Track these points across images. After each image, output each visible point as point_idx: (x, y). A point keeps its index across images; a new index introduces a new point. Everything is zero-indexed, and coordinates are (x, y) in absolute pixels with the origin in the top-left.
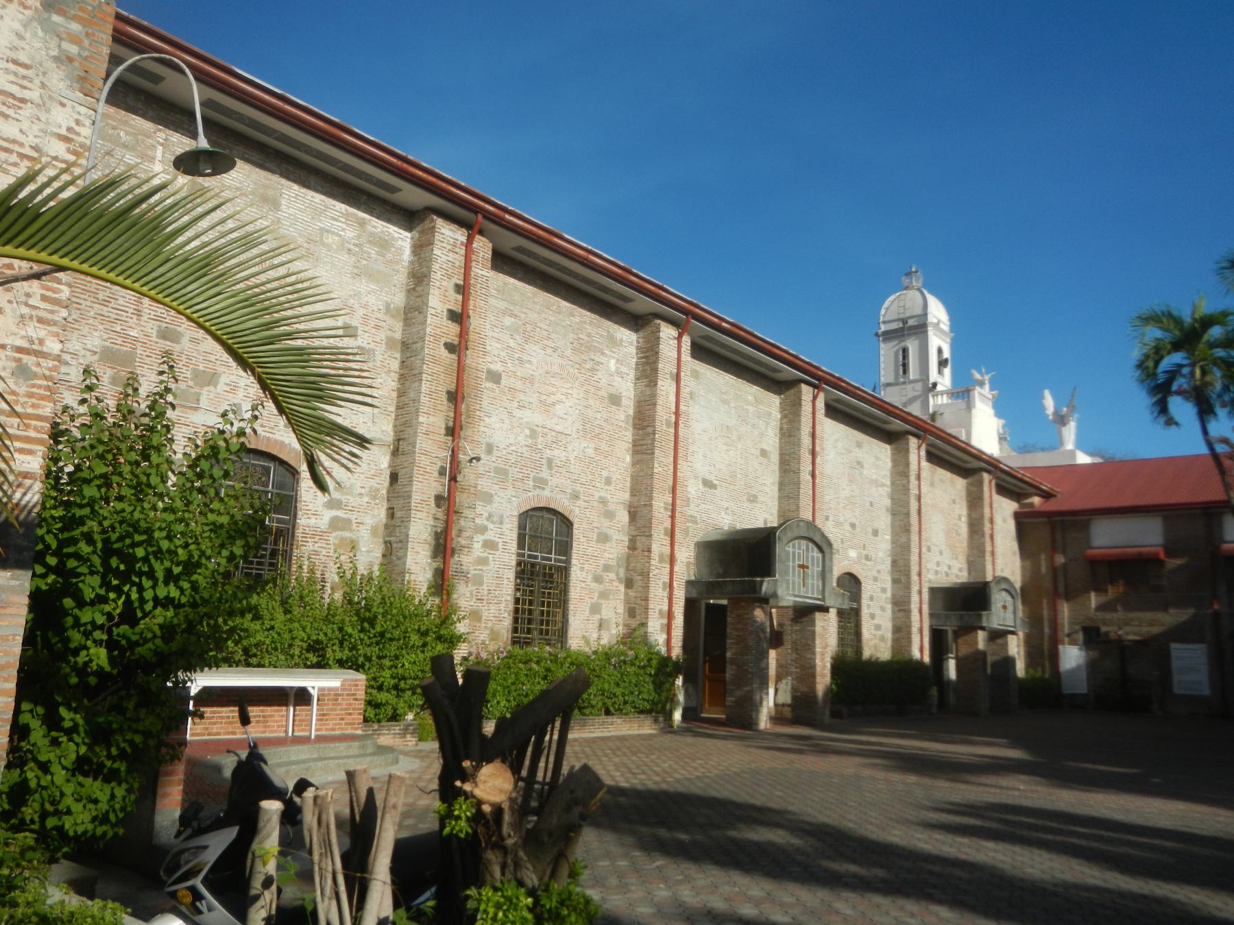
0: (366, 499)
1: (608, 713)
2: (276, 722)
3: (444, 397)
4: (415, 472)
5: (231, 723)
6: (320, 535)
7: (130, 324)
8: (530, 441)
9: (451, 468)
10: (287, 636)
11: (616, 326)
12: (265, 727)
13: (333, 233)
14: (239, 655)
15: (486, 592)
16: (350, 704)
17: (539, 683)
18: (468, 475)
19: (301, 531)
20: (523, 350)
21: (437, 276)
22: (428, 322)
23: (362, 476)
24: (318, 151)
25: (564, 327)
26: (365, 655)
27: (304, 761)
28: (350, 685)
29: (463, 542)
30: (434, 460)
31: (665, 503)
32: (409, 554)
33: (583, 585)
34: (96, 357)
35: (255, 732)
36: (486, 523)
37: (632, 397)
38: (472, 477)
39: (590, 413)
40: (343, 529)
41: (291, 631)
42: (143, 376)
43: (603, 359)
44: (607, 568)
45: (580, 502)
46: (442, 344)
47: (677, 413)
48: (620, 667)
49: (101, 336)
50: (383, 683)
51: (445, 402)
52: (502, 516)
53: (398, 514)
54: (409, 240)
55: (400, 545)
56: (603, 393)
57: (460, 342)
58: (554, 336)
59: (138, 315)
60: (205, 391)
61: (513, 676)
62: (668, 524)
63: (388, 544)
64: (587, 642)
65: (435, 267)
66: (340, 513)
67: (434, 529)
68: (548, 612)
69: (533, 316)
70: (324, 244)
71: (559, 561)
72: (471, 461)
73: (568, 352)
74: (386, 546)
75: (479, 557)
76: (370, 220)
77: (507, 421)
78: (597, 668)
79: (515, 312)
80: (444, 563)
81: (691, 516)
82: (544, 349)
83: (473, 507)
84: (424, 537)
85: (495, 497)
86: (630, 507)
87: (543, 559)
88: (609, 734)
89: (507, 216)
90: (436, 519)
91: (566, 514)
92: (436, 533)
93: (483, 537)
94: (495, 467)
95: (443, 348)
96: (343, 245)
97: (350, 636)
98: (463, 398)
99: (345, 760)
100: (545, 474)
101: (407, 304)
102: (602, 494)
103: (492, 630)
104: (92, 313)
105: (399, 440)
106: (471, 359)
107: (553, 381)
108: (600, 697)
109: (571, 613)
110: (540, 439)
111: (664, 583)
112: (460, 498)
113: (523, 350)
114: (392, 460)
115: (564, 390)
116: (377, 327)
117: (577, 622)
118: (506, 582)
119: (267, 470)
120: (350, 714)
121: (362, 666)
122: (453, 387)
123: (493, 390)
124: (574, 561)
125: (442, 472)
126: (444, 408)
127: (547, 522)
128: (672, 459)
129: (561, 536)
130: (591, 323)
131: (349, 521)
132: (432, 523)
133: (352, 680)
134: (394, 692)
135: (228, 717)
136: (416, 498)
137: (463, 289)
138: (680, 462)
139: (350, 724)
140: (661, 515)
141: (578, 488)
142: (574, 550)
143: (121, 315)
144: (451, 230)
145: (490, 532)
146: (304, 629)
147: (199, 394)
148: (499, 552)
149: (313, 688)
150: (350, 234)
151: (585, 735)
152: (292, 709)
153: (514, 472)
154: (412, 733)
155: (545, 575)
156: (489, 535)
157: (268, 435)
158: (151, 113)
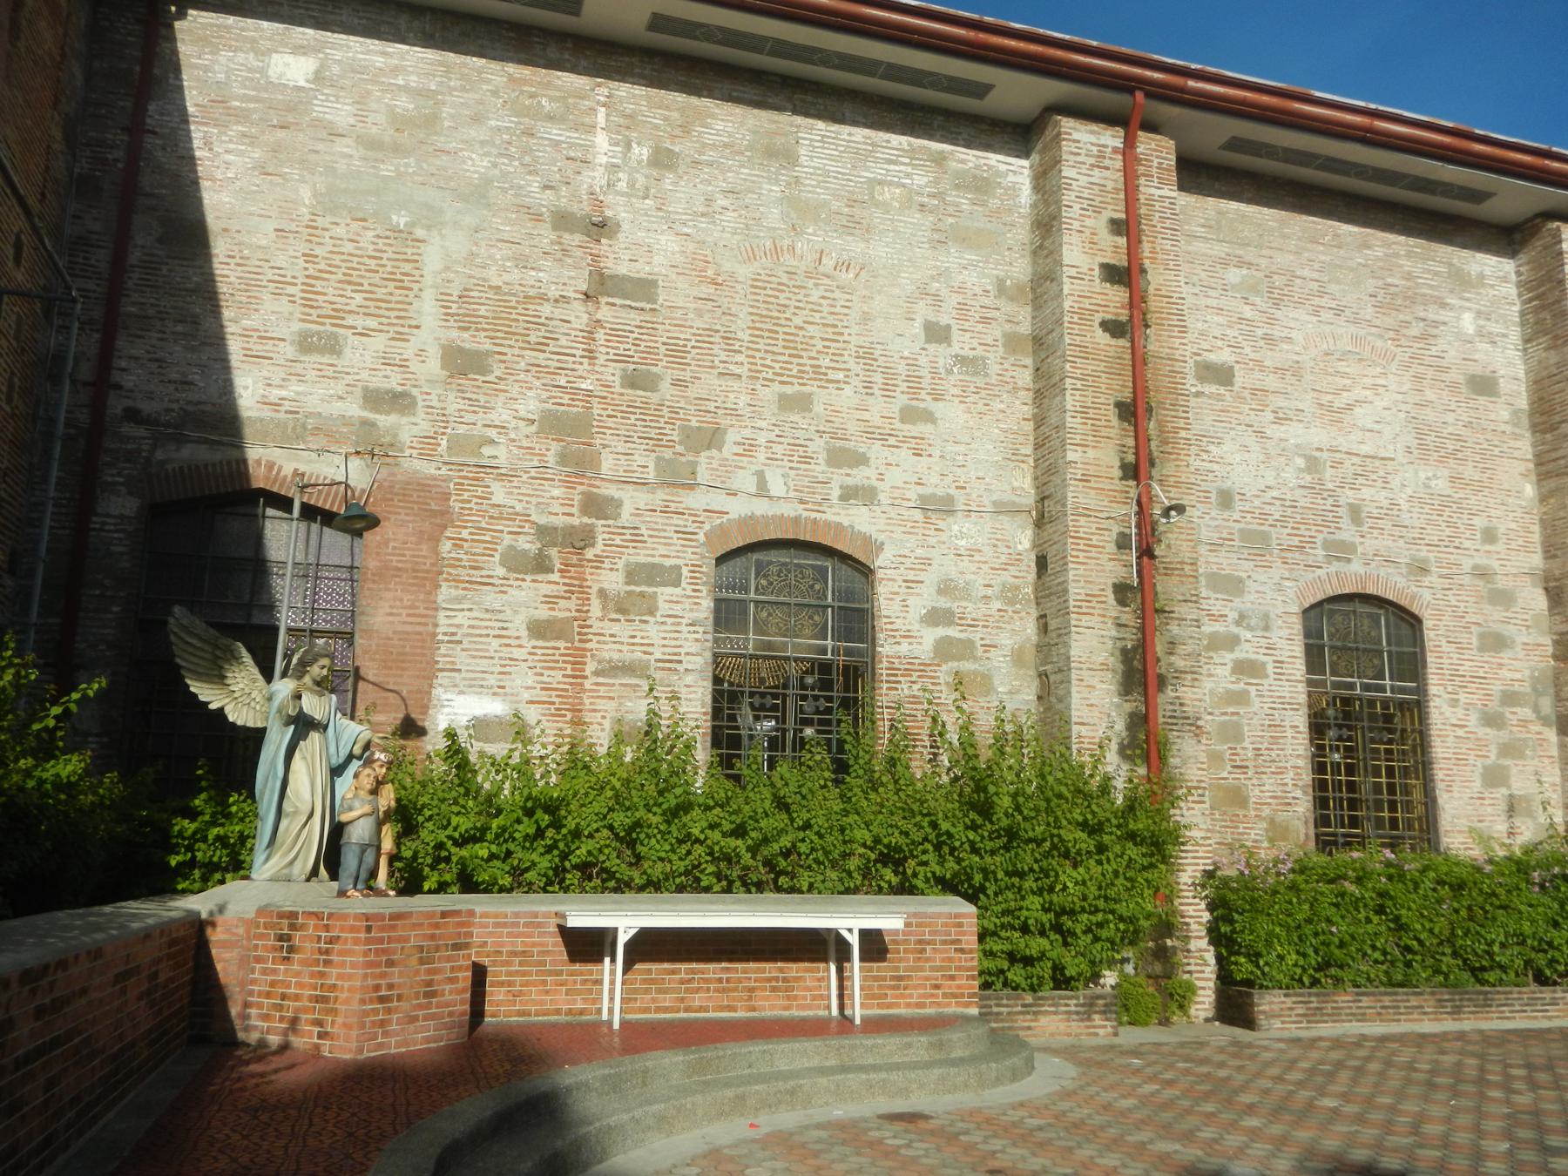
0: (997, 605)
1: (1541, 980)
2: (809, 989)
3: (1112, 413)
4: (1069, 546)
5: (724, 990)
7: (579, 373)
8: (1308, 478)
9: (1139, 534)
10: (832, 839)
11: (1466, 253)
12: (788, 998)
13: (890, 184)
14: (763, 873)
15: (1250, 754)
16: (950, 960)
17: (1369, 921)
18: (1174, 542)
19: (885, 665)
20: (1272, 321)
21: (1073, 210)
22: (1066, 291)
23: (985, 567)
24: (838, 55)
25: (1352, 269)
26: (985, 871)
27: (796, 1074)
28: (946, 925)
29: (1180, 663)
30: (1105, 524)
32: (1074, 689)
33: (1460, 732)
34: (534, 428)
35: (772, 1007)
36: (1235, 630)
37: (1522, 374)
38: (1185, 546)
39: (1429, 415)
40: (960, 658)
41: (842, 830)
42: (604, 446)
43: (1445, 315)
44: (1510, 698)
46: (1096, 324)
48: (1557, 889)
49: (539, 395)
50: (1027, 918)
51: (1115, 421)
52: (1266, 617)
53: (1053, 624)
54: (1026, 172)
55: (1059, 677)
56: (1454, 376)
57: (1131, 317)
58: (1332, 288)
59: (590, 358)
60: (703, 458)
61: (1306, 907)
63: (1043, 675)
64: (1484, 840)
65: (1068, 197)
66: (953, 632)
67: (1119, 644)
68: (1391, 789)
69: (1283, 260)
70: (877, 204)
71: (1403, 690)
72: (1166, 512)
73: (1369, 312)
74: (1042, 682)
75: (1228, 691)
76: (952, 153)
77: (1255, 448)
78: (1500, 891)
79: (1249, 258)
80: (1146, 703)
82: (1316, 313)
83: (1195, 600)
84: (1101, 659)
85: (1249, 583)
86: (1546, 580)
87: (1366, 688)
88: (1545, 1024)
89: (1191, 83)
91: (1403, 602)
92: (1124, 651)
94: (1241, 531)
95: (1099, 331)
96: (912, 201)
97: (949, 835)
98: (1150, 410)
99: (884, 1075)
100: (1348, 533)
101: (1034, 274)
102: (1480, 560)
103: (1272, 822)
104: (522, 365)
105: (1043, 499)
106: (1156, 342)
107: (1342, 367)
108: (1517, 949)
109: (1440, 787)
110: (1329, 473)
112: (1166, 587)
113: (1272, 321)
114: (1037, 535)
115: (1368, 381)
116: (985, 320)
118: (1290, 733)
119: (822, 572)
120: (952, 978)
121: (983, 889)
122: (1127, 395)
123: (1219, 397)
124: (1433, 690)
125: (1122, 543)
126: (1113, 433)
127: (1366, 622)
129: (1399, 644)
130: (1409, 255)
131: (969, 644)
132: (1114, 633)
133: (950, 916)
134: (1053, 936)
135: (720, 980)
136: (1076, 591)
137: (1127, 227)
139: (955, 996)
141: (1423, 554)
142: (1431, 669)
143: (566, 362)
144: (1092, 132)
146: (867, 825)
147: (694, 464)
149: (850, 930)
150: (920, 179)
151: (1485, 1025)
152: (833, 968)
153: (1280, 535)
154: (1104, 1012)
155: (1373, 717)
156: (1245, 652)
157: (814, 515)
158: (584, 63)
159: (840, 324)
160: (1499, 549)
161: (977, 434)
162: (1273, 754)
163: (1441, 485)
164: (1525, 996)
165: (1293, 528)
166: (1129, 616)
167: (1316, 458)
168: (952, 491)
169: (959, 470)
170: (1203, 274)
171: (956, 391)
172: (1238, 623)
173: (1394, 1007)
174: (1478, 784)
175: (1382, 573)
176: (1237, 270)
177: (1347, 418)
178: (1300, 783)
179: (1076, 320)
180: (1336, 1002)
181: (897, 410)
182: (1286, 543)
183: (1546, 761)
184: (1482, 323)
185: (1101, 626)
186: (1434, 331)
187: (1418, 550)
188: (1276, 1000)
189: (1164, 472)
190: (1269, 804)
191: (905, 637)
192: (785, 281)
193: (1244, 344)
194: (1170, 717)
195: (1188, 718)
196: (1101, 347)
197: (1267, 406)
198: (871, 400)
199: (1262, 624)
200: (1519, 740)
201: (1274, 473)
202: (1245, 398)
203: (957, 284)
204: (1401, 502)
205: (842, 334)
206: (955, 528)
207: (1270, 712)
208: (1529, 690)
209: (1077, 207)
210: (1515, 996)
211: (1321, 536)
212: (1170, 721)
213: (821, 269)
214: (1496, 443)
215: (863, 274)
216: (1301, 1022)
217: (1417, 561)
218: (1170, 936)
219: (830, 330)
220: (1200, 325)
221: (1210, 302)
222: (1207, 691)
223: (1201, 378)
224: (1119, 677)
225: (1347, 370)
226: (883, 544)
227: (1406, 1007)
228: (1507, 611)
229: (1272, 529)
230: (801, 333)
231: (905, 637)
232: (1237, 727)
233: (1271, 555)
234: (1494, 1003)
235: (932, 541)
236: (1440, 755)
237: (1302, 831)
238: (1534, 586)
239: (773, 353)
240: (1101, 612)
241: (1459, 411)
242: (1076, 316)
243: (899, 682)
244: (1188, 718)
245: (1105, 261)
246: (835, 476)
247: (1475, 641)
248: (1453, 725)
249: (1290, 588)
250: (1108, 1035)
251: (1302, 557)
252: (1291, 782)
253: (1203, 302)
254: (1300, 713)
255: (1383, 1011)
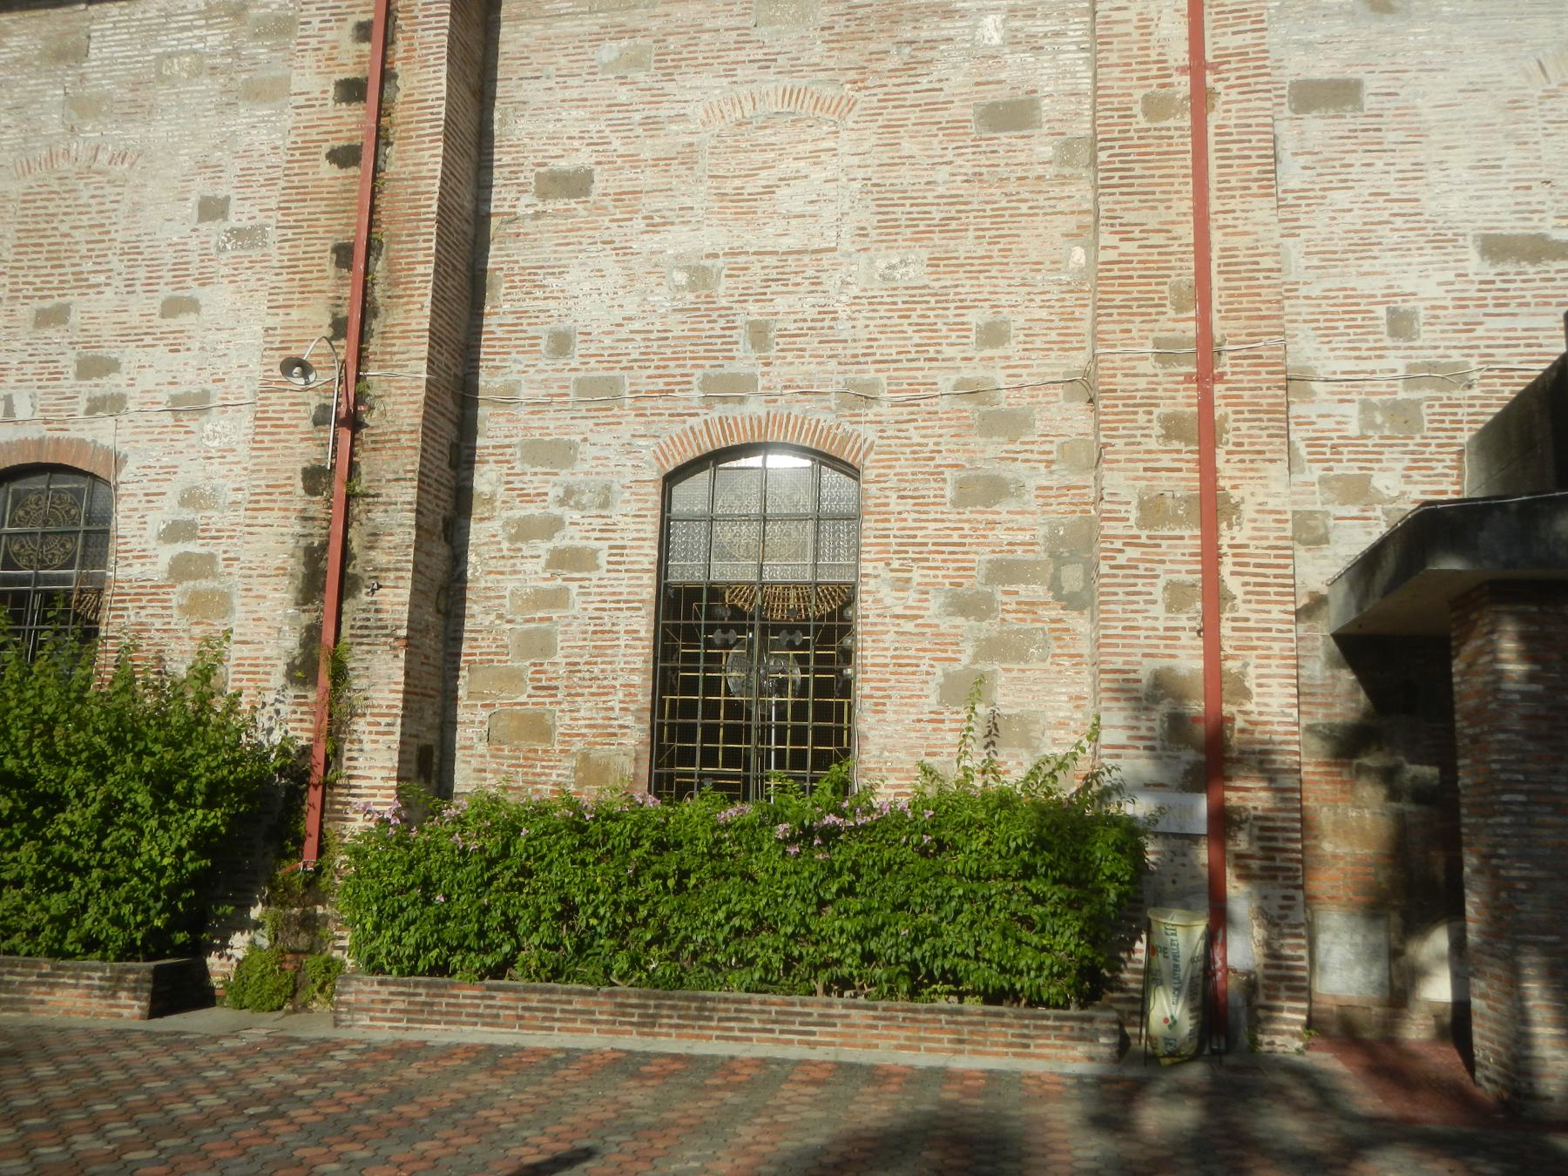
6: (151, 592)
8: (690, 297)
13: (182, 53)
20: (658, 97)
23: (237, 469)
31: (1157, 343)
36: (556, 511)
39: (906, 175)
43: (949, 28)
44: (1004, 571)
45: (884, 410)
46: (322, 157)
47: (1197, 66)
51: (331, 270)
52: (608, 488)
58: (756, 34)
62: (1184, 402)
66: (193, 547)
67: (303, 542)
75: (537, 591)
79: (631, 25)
81: (1432, 366)
84: (278, 563)
85: (586, 449)
88: (795, 1052)
90: (305, 519)
93: (550, 545)
94: (579, 381)
100: (745, 361)
102: (967, 373)
103: (585, 757)
107: (763, 137)
110: (725, 283)
111: (1171, 587)
117: (890, 729)
123: (568, 213)
125: (320, 420)
126: (326, 285)
128: (1187, 205)
131: (211, 558)
132: (298, 529)
138: (1214, 205)
140: (1142, 383)
145: (570, 530)
148: (602, 573)
159: (107, 222)
160: (1010, 353)
161: (244, 315)
162: (596, 670)
163: (916, 273)
164: (774, 1009)
165: (657, 367)
166: (319, 507)
167: (705, 269)
168: (209, 386)
169: (218, 361)
170: (563, 61)
171: (226, 271)
172: (562, 502)
173: (544, 1010)
174: (933, 700)
175: (796, 410)
176: (614, 44)
177: (763, 205)
178: (633, 707)
179: (298, 157)
180: (457, 996)
181: (158, 304)
182: (643, 389)
183: (1067, 662)
184: (1016, 24)
185: (282, 522)
186: (929, 54)
187: (862, 371)
188: (367, 989)
189: (389, 321)
190: (584, 735)
191: (138, 557)
192: (56, 188)
193: (613, 137)
194: (361, 628)
195: (385, 627)
196: (326, 182)
197: (636, 212)
198: (132, 298)
199: (598, 501)
200: (1018, 632)
201: (637, 299)
202: (606, 208)
203: (240, 149)
204: (839, 307)
205: (108, 232)
206: (208, 427)
207: (597, 614)
208: (1044, 556)
209: (316, 22)
210: (757, 1007)
211: (699, 373)
212: (359, 632)
213: (95, 166)
214: (1026, 196)
215: (140, 160)
216: (400, 1020)
217: (855, 387)
218: (322, 902)
219: (96, 231)
220: (550, 127)
221: (568, 94)
222: (507, 593)
223: (543, 195)
224: (298, 583)
225: (773, 139)
226: (126, 456)
227: (563, 1011)
228: (1012, 441)
229: (625, 373)
230: (66, 240)
231: (138, 557)
232: (548, 635)
233: (621, 407)
234: (716, 1016)
235: (179, 446)
236: (869, 661)
237: (630, 769)
238: (1070, 398)
239: (36, 268)
240: (282, 505)
241: (959, 161)
242: (297, 153)
243: (126, 609)
244: (385, 627)
245: (343, 77)
246: (83, 390)
247: (949, 492)
248: (897, 617)
249: (647, 447)
250: (133, 1017)
251: (669, 404)
252: (617, 706)
253: (560, 95)
254: (642, 613)
255: (527, 1014)
